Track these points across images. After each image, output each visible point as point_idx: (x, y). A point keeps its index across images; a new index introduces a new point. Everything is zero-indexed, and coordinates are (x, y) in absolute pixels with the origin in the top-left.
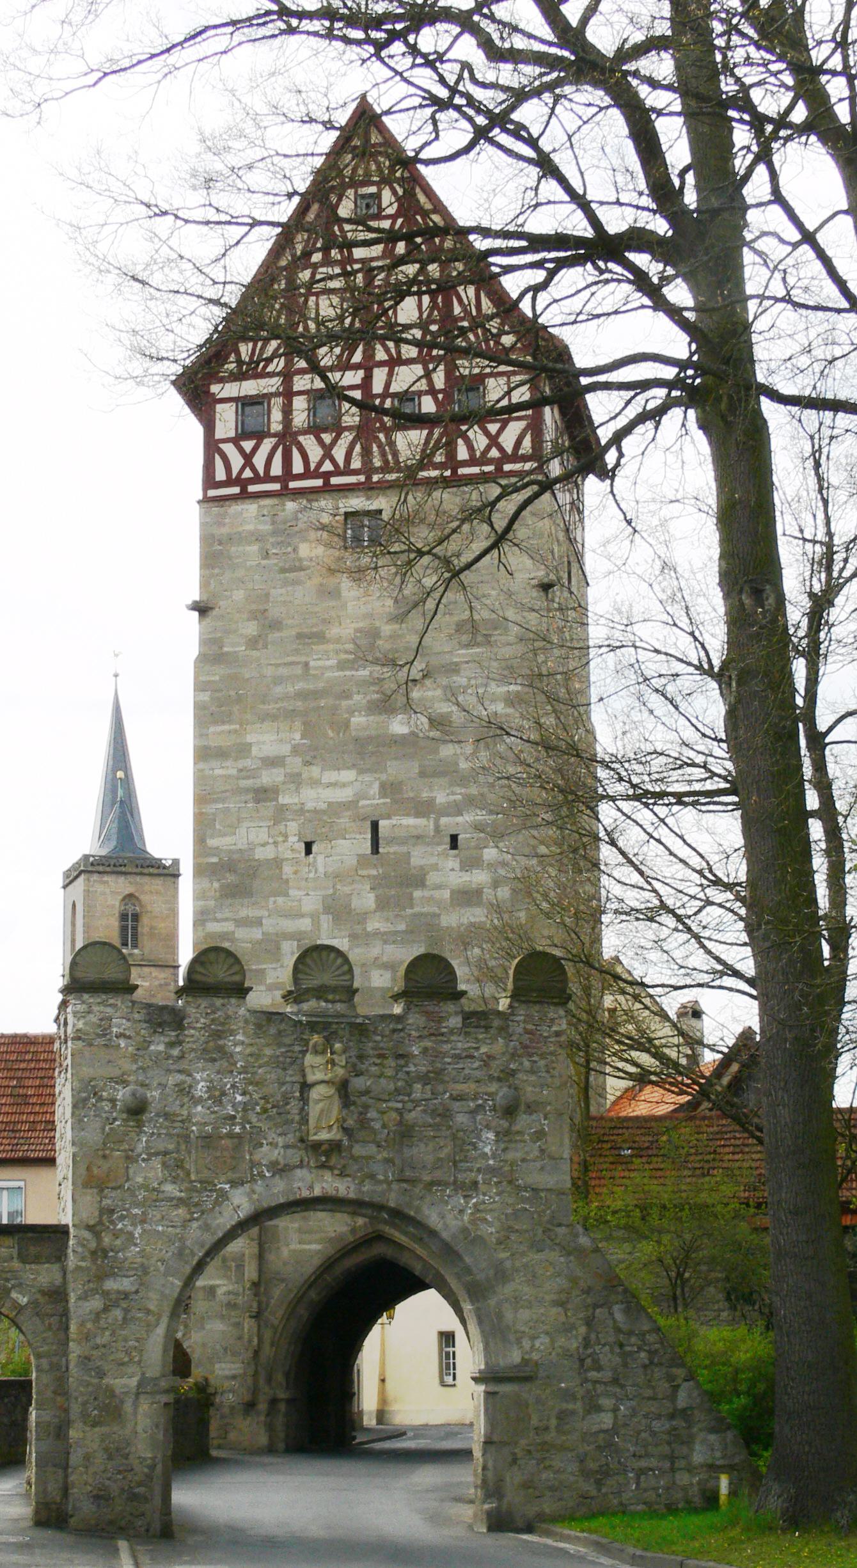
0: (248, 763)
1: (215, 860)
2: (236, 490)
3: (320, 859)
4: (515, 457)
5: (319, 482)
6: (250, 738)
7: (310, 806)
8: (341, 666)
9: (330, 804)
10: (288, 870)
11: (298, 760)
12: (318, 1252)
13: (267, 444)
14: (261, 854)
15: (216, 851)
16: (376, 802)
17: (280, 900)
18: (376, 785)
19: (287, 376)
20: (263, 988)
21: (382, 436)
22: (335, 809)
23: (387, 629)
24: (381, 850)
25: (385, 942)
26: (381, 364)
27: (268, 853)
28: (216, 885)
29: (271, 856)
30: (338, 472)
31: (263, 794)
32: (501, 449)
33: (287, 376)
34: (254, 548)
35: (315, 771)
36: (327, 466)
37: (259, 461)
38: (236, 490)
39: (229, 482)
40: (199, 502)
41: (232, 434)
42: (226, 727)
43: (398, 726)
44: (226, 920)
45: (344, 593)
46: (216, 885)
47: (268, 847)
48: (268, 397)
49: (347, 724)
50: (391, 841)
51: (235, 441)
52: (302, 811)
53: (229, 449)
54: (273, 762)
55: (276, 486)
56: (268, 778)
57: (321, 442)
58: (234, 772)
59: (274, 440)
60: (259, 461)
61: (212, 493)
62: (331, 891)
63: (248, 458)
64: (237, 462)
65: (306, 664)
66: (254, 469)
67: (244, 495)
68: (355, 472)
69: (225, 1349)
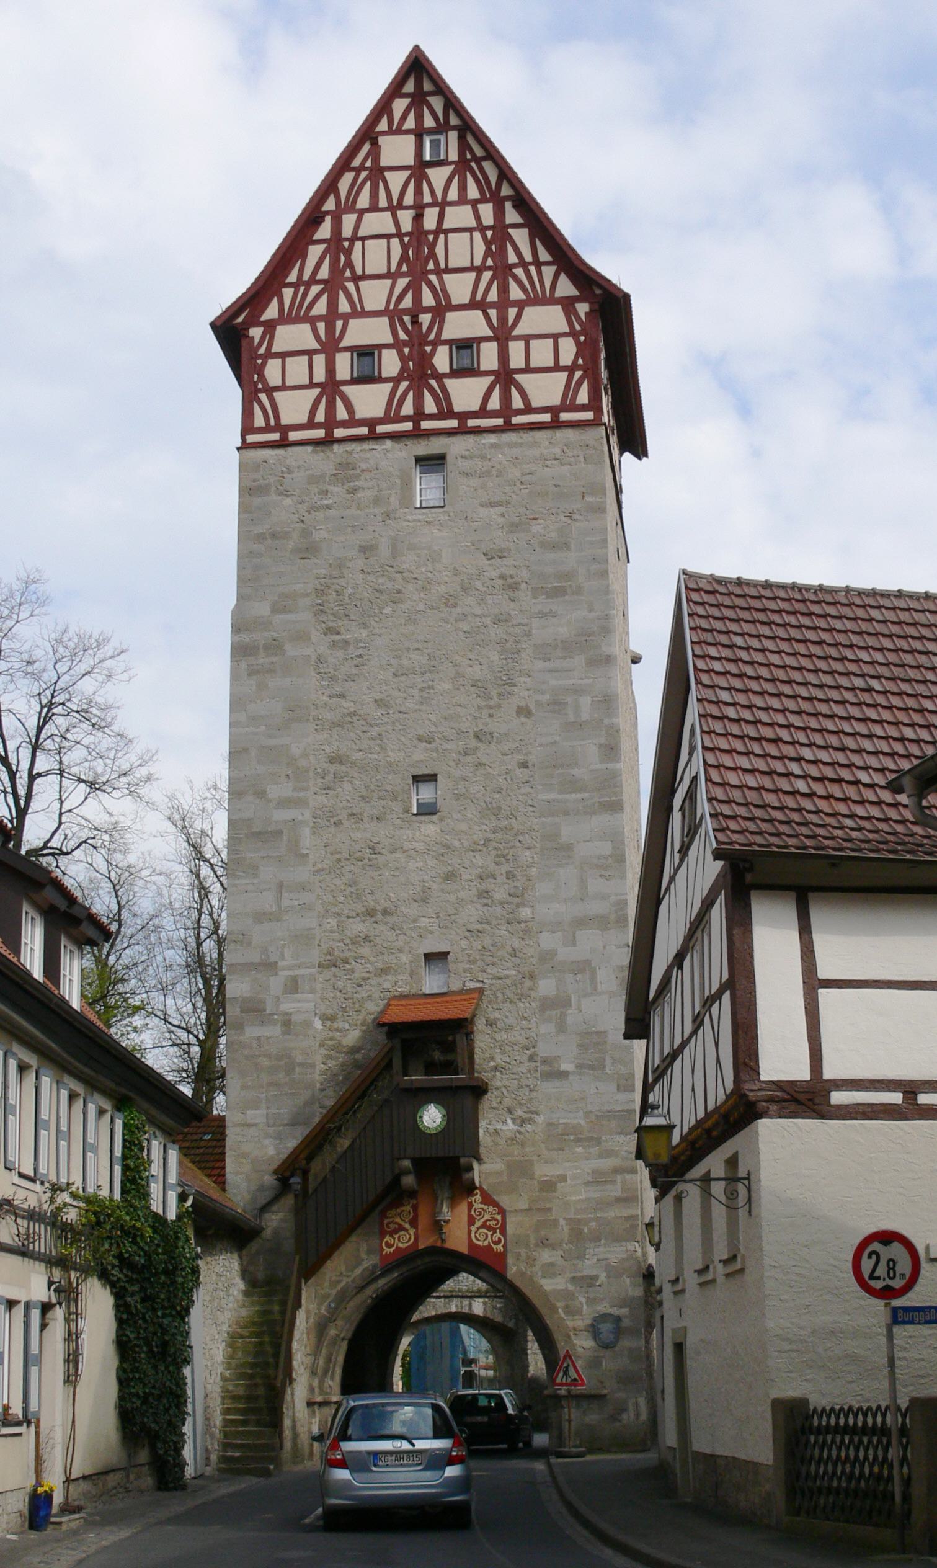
2: (275, 436)
21: (433, 382)
38: (275, 436)
39: (267, 429)
40: (238, 449)
61: (251, 438)
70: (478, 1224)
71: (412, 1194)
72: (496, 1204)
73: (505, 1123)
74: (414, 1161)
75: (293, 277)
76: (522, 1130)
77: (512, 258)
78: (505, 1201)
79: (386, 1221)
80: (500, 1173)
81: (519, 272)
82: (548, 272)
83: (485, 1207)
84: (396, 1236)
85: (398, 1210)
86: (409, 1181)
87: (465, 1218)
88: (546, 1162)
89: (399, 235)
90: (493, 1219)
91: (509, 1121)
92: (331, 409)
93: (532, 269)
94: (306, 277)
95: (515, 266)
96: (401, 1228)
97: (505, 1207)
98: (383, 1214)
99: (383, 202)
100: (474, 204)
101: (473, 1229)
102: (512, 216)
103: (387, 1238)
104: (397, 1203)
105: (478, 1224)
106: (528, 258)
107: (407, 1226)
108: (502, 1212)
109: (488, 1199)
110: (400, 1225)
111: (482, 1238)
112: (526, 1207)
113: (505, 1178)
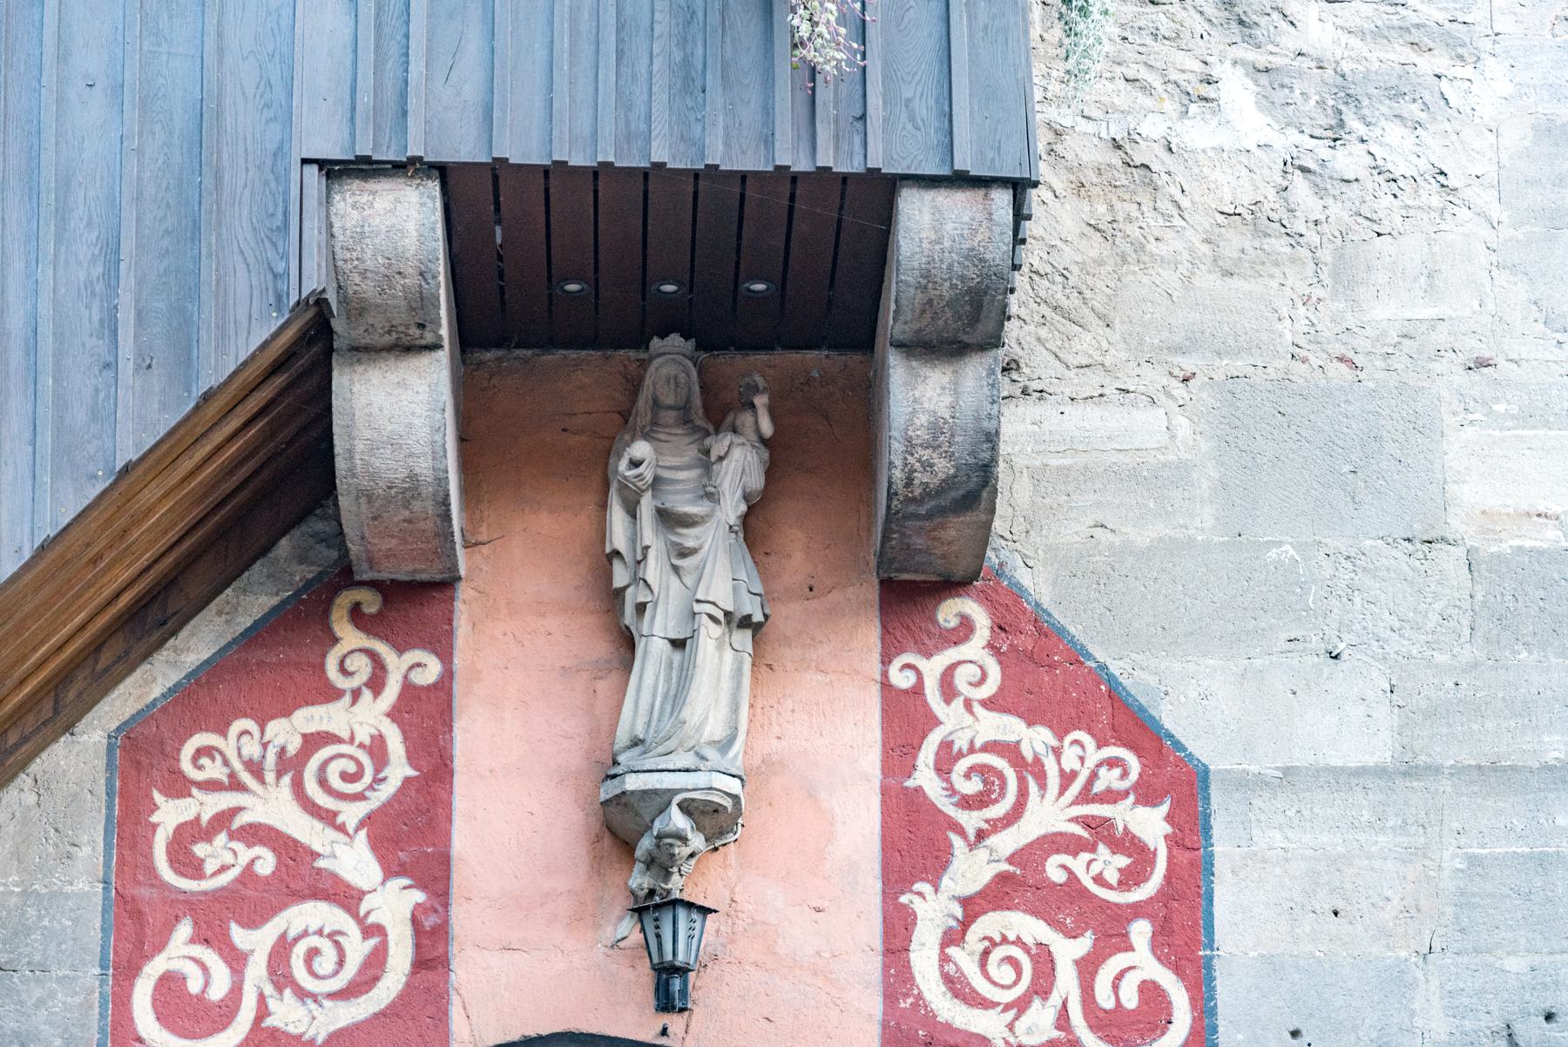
70: (971, 870)
71: (414, 601)
72: (1130, 724)
73: (1200, 95)
74: (476, 198)
76: (1348, 160)
78: (1199, 706)
79: (169, 814)
80: (1149, 480)
83: (1036, 739)
84: (256, 941)
85: (286, 732)
86: (398, 415)
87: (859, 824)
88: (1526, 418)
90: (1100, 830)
91: (1235, 89)
96: (301, 876)
97: (1201, 747)
98: (143, 760)
101: (932, 909)
103: (179, 952)
104: (276, 666)
105: (971, 870)
107: (354, 861)
108: (1177, 781)
109: (1050, 675)
110: (289, 850)
111: (1001, 982)
112: (1377, 749)
113: (1204, 522)
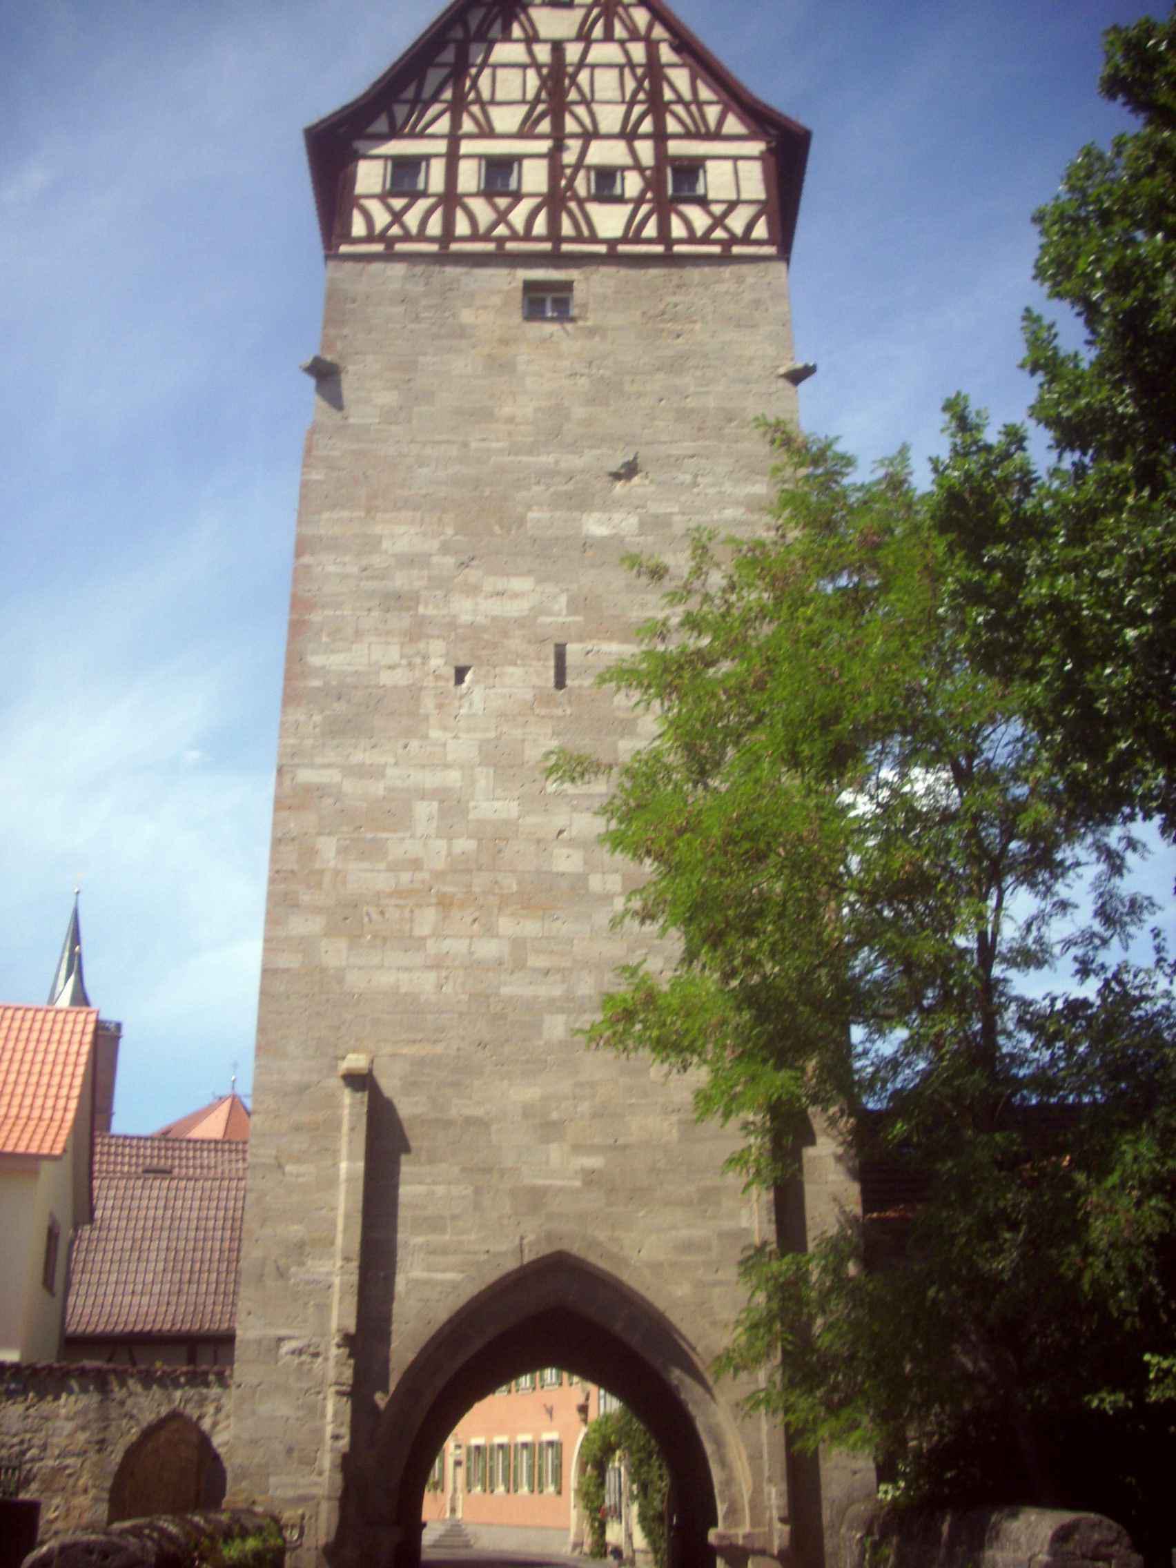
0: (376, 560)
1: (317, 683)
2: (378, 248)
3: (478, 694)
4: (746, 239)
5: (490, 247)
6: (378, 529)
7: (465, 618)
8: (514, 450)
9: (494, 619)
10: (428, 704)
11: (450, 561)
12: (455, 1286)
13: (422, 205)
14: (386, 678)
15: (322, 671)
16: (561, 619)
17: (414, 744)
18: (563, 599)
19: (454, 138)
20: (382, 866)
21: (573, 205)
22: (503, 627)
23: (579, 412)
24: (568, 682)
25: (575, 809)
26: (573, 136)
27: (400, 678)
28: (317, 718)
29: (403, 682)
30: (514, 237)
31: (399, 601)
32: (727, 229)
33: (454, 138)
34: (400, 309)
35: (473, 575)
36: (501, 230)
37: (412, 219)
38: (378, 248)
39: (370, 238)
41: (377, 189)
42: (345, 514)
43: (595, 526)
44: (329, 766)
45: (521, 368)
46: (317, 718)
47: (399, 671)
48: (427, 158)
49: (522, 521)
50: (583, 671)
51: (383, 197)
52: (452, 625)
53: (374, 207)
54: (410, 561)
55: (434, 248)
56: (400, 581)
57: (495, 207)
58: (355, 570)
59: (431, 201)
60: (412, 219)
61: (344, 249)
62: (492, 735)
63: (397, 217)
64: (381, 218)
65: (465, 445)
66: (403, 226)
67: (390, 256)
68: (539, 239)
69: (290, 1451)
75: (410, 93)
77: (668, 95)
81: (679, 109)
82: (712, 113)
89: (538, 67)
92: (449, 223)
93: (693, 108)
94: (427, 93)
95: (671, 102)
99: (517, 31)
100: (622, 42)
102: (666, 54)
106: (687, 94)
